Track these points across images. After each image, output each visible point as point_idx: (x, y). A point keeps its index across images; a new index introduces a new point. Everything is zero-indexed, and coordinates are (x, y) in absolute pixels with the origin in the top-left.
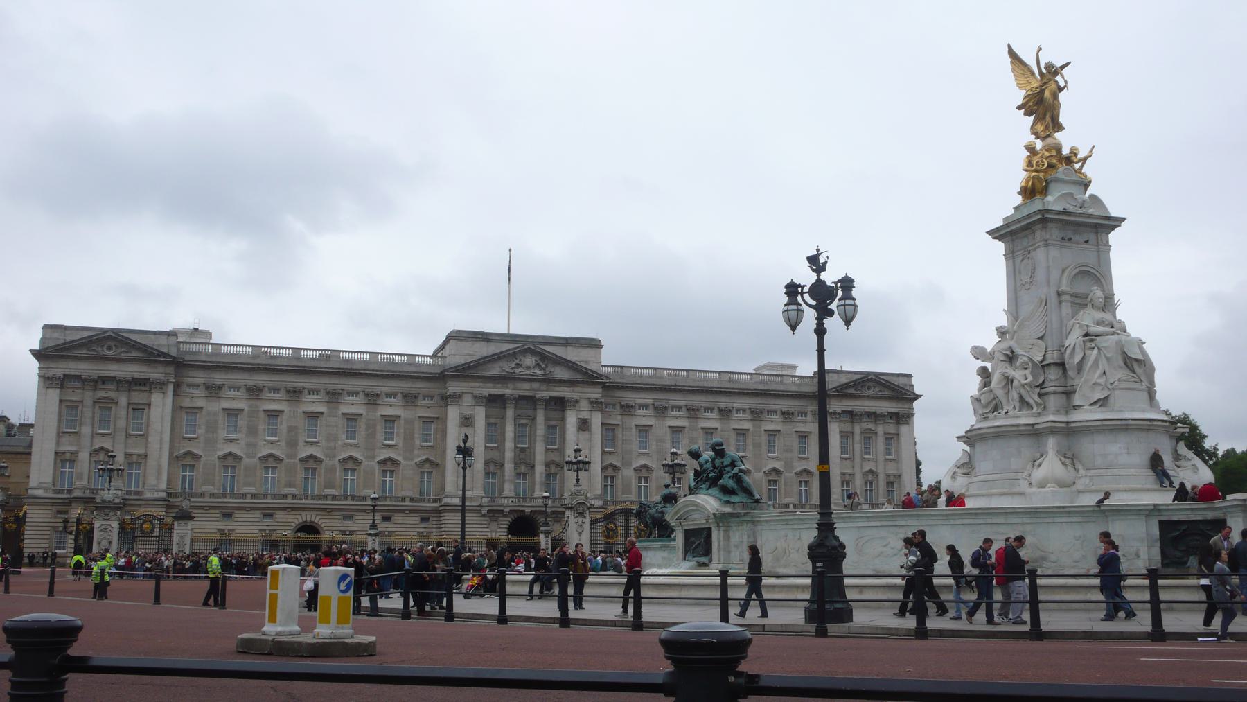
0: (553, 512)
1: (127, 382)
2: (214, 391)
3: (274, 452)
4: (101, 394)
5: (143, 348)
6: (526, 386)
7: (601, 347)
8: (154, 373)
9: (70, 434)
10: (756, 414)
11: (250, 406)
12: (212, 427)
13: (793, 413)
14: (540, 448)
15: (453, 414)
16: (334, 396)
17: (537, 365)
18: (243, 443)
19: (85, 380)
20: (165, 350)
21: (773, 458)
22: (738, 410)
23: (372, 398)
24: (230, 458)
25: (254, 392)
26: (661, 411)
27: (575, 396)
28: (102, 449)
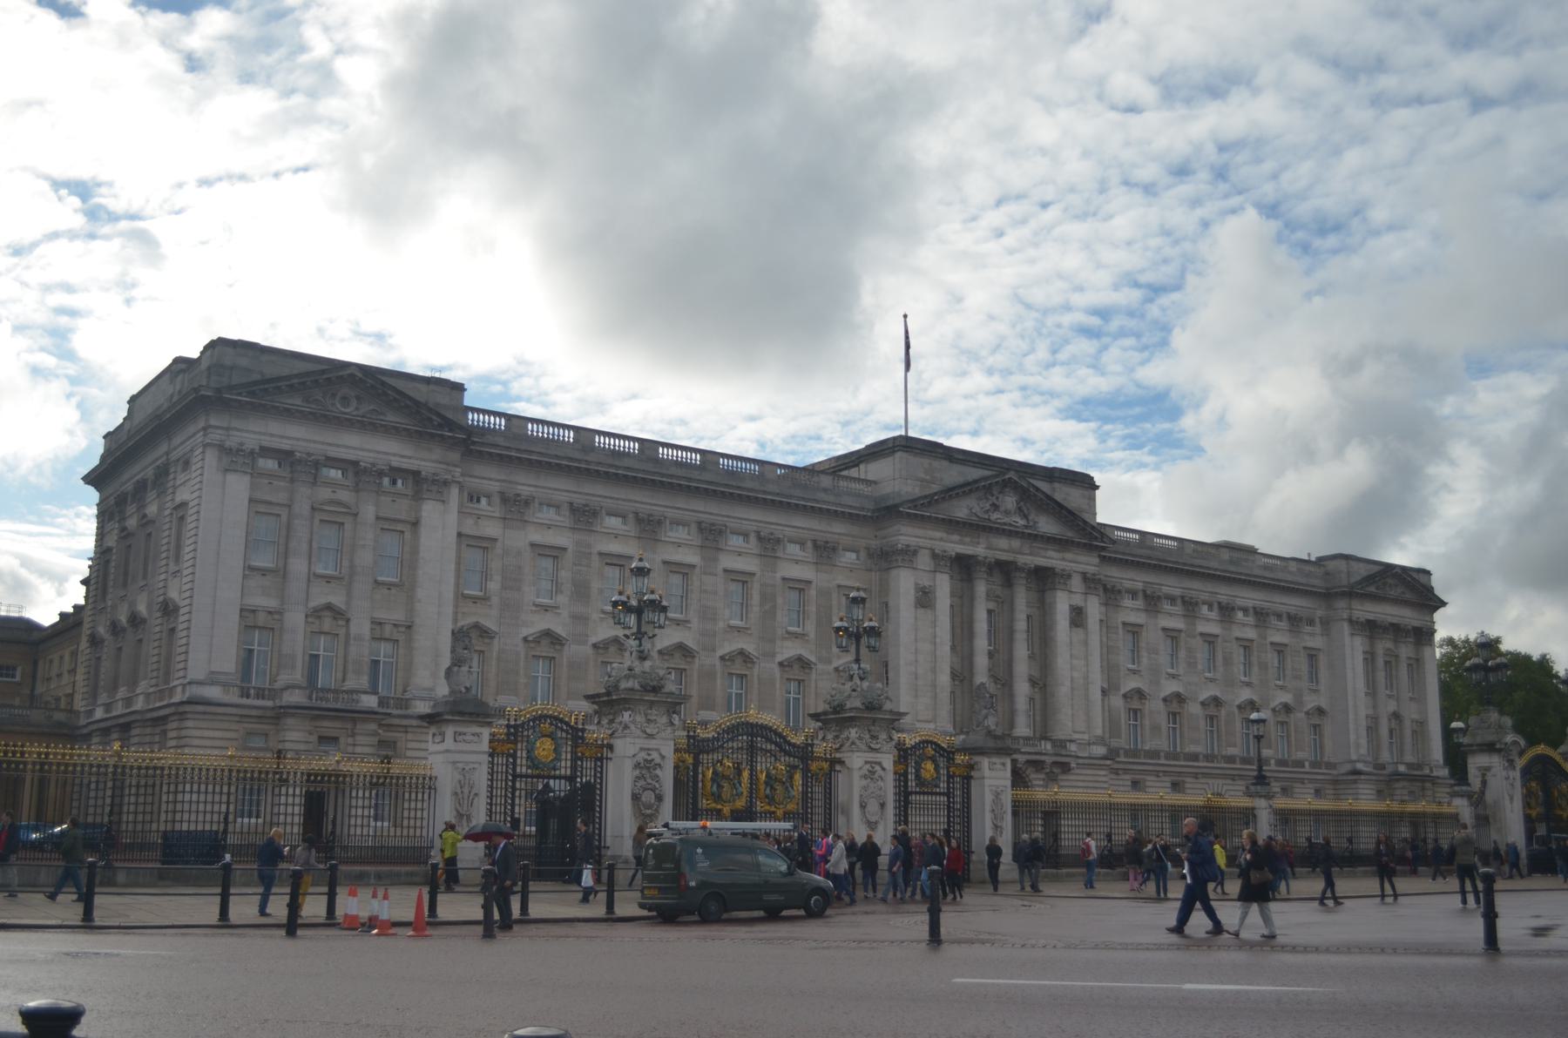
0: (1055, 763)
1: (381, 474)
2: (515, 507)
4: (324, 493)
6: (1003, 543)
8: (426, 459)
9: (264, 572)
10: (1261, 616)
14: (1021, 651)
15: (905, 583)
16: (711, 535)
19: (300, 461)
23: (769, 545)
24: (545, 642)
26: (1152, 602)
28: (328, 607)
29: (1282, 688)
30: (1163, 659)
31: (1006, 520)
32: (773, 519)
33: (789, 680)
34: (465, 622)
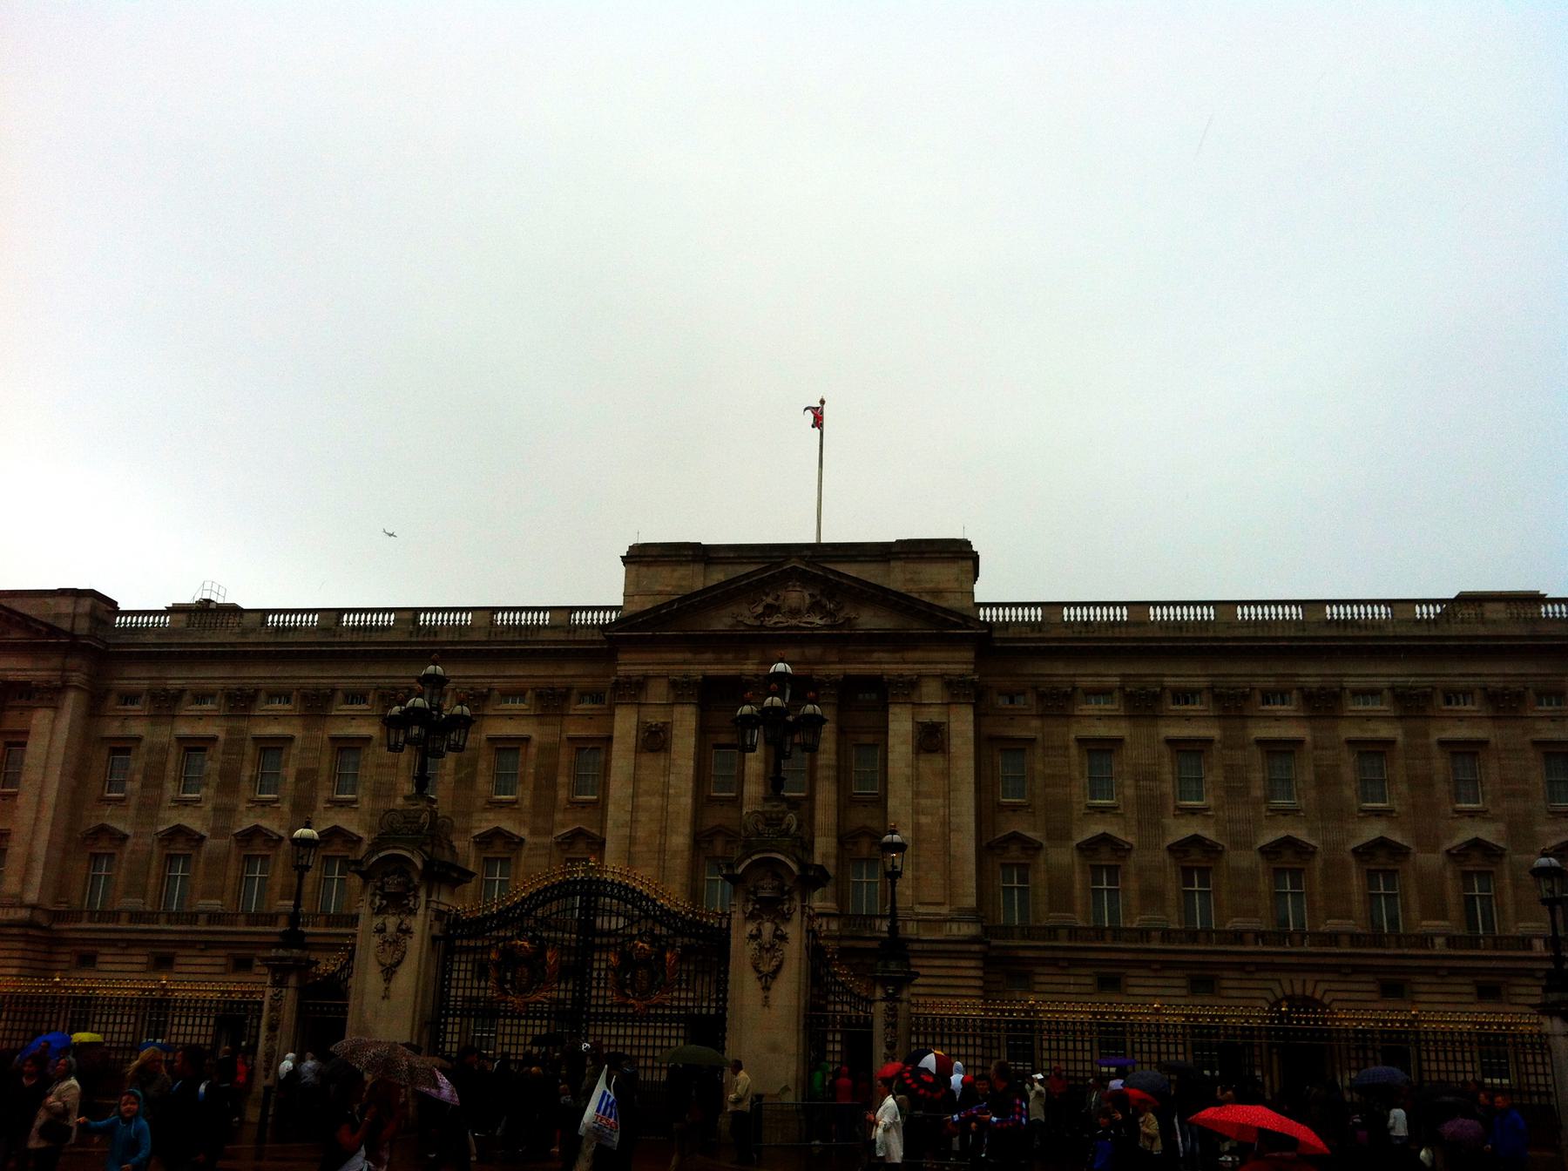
2: (165, 704)
3: (265, 824)
5: (25, 621)
7: (975, 558)
10: (1411, 704)
11: (228, 732)
12: (153, 778)
13: (1519, 697)
14: (826, 794)
17: (815, 607)
18: (208, 807)
20: (65, 625)
21: (1472, 814)
22: (1358, 693)
25: (241, 702)
26: (1143, 705)
27: (907, 670)
29: (1472, 814)
30: (1168, 788)
31: (794, 622)
32: (481, 673)
33: (486, 859)
34: (94, 823)
